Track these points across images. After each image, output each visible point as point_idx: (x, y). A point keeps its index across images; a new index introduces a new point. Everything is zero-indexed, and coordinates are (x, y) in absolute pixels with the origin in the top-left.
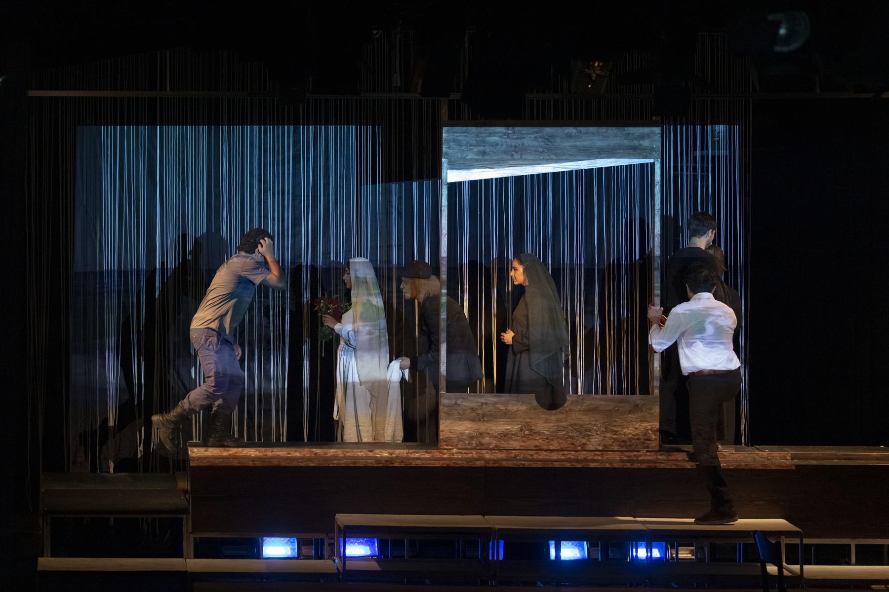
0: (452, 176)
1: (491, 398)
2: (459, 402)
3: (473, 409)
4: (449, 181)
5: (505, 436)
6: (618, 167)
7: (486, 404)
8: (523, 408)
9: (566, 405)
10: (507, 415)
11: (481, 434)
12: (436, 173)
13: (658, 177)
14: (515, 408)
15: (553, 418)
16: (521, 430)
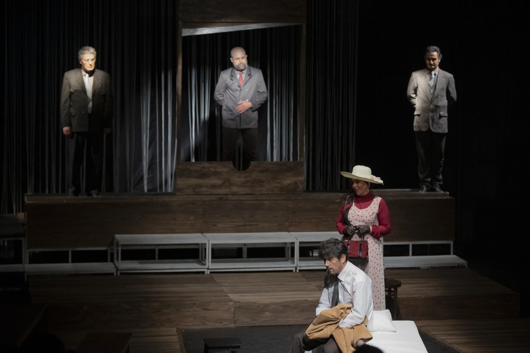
0: (186, 32)
1: (206, 164)
2: (188, 167)
3: (196, 171)
4: (183, 35)
5: (214, 186)
7: (204, 168)
8: (225, 170)
9: (250, 167)
10: (216, 174)
11: (200, 186)
12: (175, 32)
13: (304, 33)
14: (220, 170)
15: (243, 175)
16: (224, 183)
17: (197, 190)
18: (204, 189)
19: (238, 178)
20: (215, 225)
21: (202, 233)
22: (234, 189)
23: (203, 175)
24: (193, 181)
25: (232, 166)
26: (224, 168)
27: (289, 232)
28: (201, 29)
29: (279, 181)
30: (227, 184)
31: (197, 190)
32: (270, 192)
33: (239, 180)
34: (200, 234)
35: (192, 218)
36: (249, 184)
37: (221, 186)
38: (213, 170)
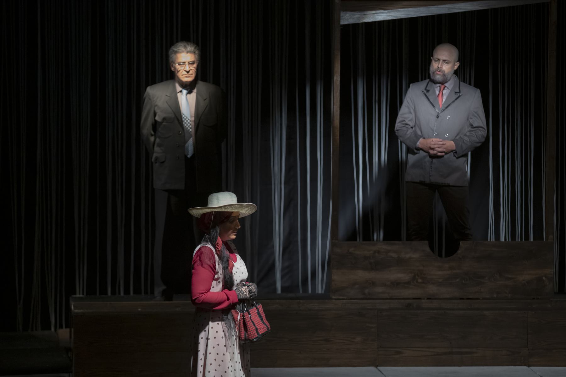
0: (348, 18)
2: (351, 250)
4: (342, 23)
5: (396, 284)
6: (513, 7)
7: (379, 252)
8: (416, 256)
9: (459, 252)
14: (408, 256)
17: (366, 291)
18: (379, 289)
19: (438, 269)
20: (399, 353)
21: (376, 366)
22: (432, 289)
23: (377, 265)
24: (361, 275)
25: (428, 249)
26: (415, 252)
27: (529, 366)
28: (374, 12)
29: (510, 276)
30: (420, 281)
31: (366, 291)
32: (495, 296)
33: (440, 273)
34: (372, 369)
35: (358, 339)
36: (458, 280)
37: (408, 283)
38: (394, 255)
